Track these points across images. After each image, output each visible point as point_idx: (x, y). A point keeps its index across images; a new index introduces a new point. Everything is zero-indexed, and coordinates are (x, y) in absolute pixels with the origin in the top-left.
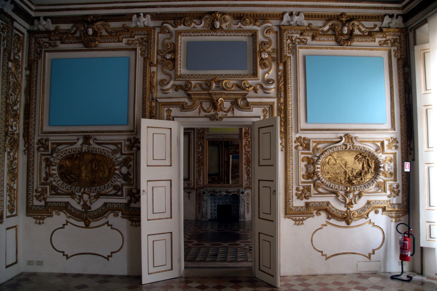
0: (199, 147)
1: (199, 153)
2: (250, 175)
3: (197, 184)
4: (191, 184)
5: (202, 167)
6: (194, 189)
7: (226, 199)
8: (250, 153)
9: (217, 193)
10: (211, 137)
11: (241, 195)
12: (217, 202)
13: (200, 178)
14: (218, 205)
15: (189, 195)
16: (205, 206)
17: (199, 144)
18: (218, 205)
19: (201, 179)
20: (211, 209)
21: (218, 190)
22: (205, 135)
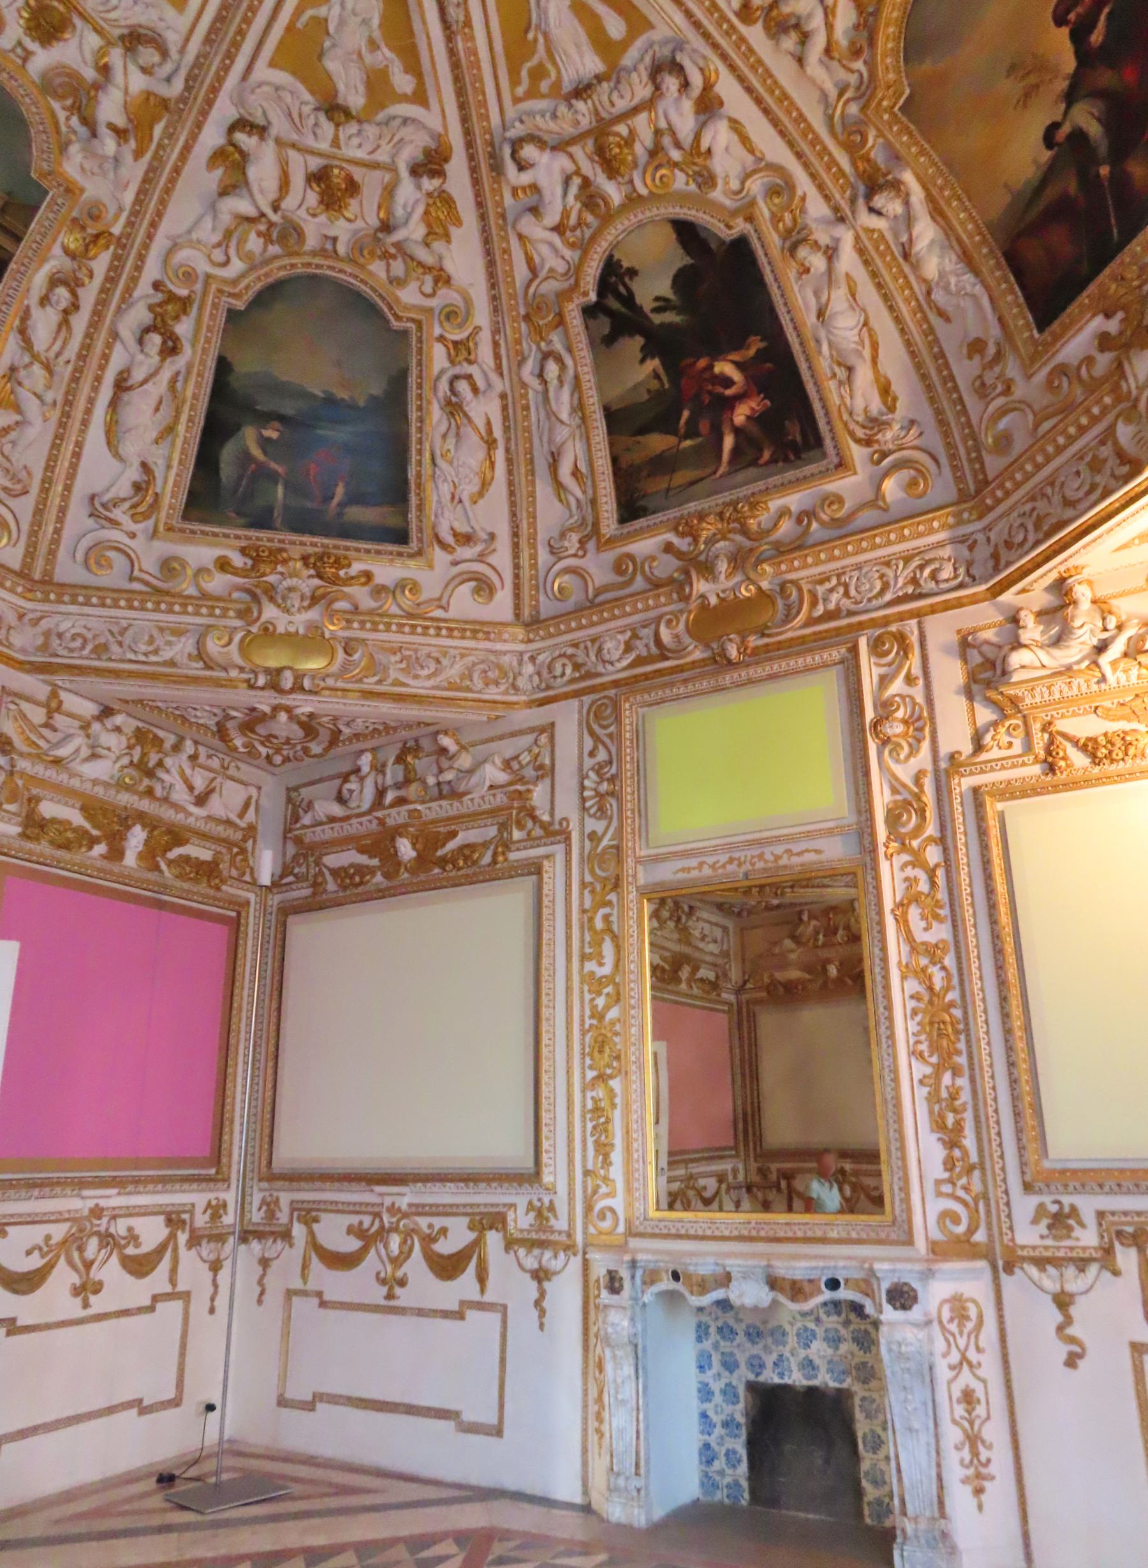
0: (598, 943)
1: (596, 984)
2: (969, 1141)
3: (588, 1208)
4: (552, 1208)
5: (615, 1084)
6: (570, 1248)
8: (949, 961)
10: (667, 873)
11: (889, 1314)
12: (742, 1358)
13: (607, 1162)
14: (752, 1387)
15: (542, 1294)
17: (599, 924)
18: (752, 1387)
19: (616, 1172)
20: (704, 1415)
22: (630, 861)
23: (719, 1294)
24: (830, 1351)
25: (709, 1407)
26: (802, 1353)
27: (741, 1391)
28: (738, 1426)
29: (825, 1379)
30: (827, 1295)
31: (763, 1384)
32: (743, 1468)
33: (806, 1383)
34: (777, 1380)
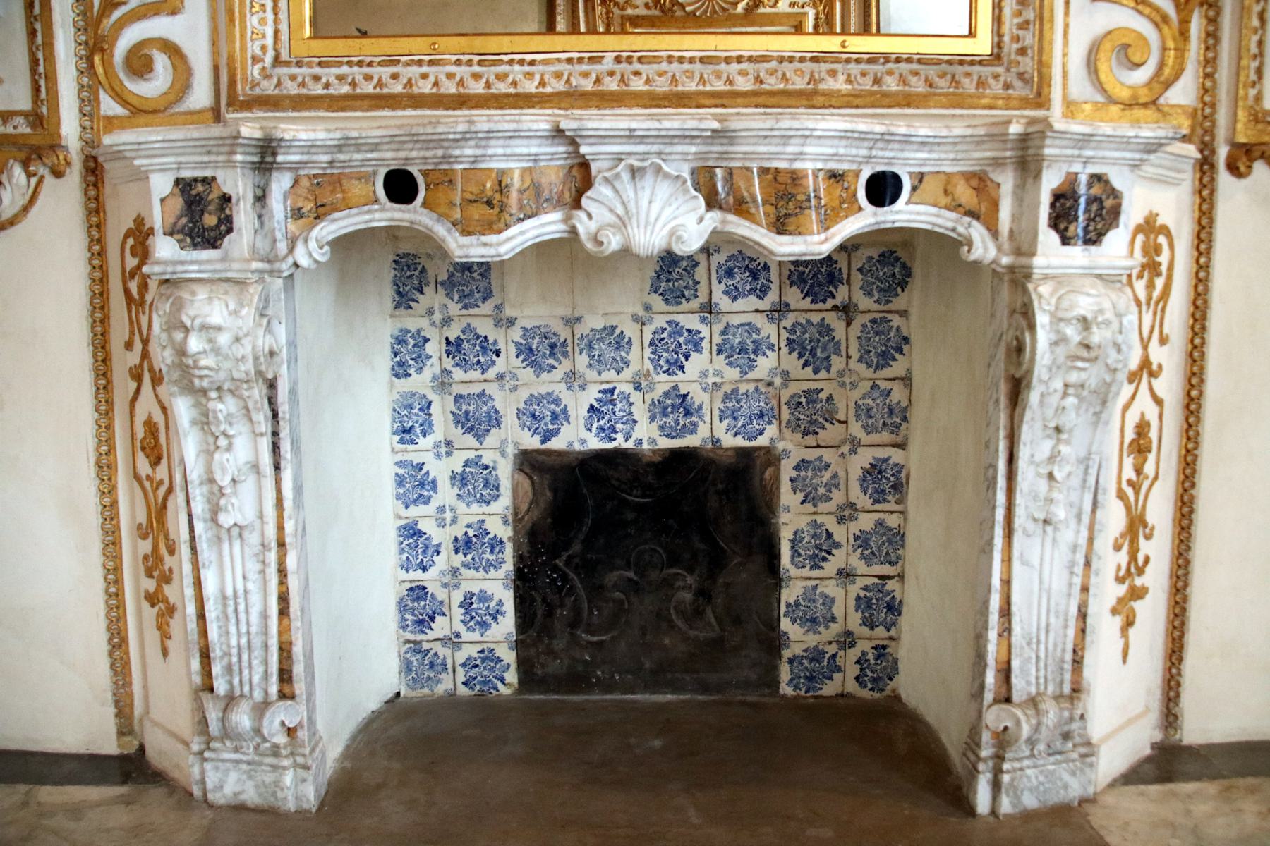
7: (673, 350)
9: (491, 205)
11: (1051, 253)
12: (507, 404)
14: (528, 462)
16: (243, 506)
18: (528, 462)
20: (411, 532)
21: (516, 146)
23: (548, 225)
24: (733, 374)
25: (424, 516)
26: (663, 382)
27: (505, 472)
28: (496, 544)
29: (713, 431)
30: (866, 218)
31: (559, 453)
32: (507, 625)
33: (665, 443)
34: (595, 443)
